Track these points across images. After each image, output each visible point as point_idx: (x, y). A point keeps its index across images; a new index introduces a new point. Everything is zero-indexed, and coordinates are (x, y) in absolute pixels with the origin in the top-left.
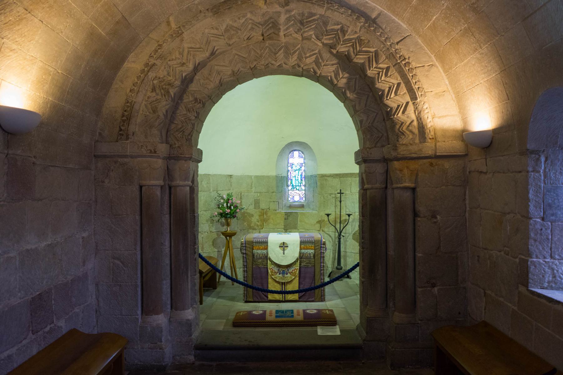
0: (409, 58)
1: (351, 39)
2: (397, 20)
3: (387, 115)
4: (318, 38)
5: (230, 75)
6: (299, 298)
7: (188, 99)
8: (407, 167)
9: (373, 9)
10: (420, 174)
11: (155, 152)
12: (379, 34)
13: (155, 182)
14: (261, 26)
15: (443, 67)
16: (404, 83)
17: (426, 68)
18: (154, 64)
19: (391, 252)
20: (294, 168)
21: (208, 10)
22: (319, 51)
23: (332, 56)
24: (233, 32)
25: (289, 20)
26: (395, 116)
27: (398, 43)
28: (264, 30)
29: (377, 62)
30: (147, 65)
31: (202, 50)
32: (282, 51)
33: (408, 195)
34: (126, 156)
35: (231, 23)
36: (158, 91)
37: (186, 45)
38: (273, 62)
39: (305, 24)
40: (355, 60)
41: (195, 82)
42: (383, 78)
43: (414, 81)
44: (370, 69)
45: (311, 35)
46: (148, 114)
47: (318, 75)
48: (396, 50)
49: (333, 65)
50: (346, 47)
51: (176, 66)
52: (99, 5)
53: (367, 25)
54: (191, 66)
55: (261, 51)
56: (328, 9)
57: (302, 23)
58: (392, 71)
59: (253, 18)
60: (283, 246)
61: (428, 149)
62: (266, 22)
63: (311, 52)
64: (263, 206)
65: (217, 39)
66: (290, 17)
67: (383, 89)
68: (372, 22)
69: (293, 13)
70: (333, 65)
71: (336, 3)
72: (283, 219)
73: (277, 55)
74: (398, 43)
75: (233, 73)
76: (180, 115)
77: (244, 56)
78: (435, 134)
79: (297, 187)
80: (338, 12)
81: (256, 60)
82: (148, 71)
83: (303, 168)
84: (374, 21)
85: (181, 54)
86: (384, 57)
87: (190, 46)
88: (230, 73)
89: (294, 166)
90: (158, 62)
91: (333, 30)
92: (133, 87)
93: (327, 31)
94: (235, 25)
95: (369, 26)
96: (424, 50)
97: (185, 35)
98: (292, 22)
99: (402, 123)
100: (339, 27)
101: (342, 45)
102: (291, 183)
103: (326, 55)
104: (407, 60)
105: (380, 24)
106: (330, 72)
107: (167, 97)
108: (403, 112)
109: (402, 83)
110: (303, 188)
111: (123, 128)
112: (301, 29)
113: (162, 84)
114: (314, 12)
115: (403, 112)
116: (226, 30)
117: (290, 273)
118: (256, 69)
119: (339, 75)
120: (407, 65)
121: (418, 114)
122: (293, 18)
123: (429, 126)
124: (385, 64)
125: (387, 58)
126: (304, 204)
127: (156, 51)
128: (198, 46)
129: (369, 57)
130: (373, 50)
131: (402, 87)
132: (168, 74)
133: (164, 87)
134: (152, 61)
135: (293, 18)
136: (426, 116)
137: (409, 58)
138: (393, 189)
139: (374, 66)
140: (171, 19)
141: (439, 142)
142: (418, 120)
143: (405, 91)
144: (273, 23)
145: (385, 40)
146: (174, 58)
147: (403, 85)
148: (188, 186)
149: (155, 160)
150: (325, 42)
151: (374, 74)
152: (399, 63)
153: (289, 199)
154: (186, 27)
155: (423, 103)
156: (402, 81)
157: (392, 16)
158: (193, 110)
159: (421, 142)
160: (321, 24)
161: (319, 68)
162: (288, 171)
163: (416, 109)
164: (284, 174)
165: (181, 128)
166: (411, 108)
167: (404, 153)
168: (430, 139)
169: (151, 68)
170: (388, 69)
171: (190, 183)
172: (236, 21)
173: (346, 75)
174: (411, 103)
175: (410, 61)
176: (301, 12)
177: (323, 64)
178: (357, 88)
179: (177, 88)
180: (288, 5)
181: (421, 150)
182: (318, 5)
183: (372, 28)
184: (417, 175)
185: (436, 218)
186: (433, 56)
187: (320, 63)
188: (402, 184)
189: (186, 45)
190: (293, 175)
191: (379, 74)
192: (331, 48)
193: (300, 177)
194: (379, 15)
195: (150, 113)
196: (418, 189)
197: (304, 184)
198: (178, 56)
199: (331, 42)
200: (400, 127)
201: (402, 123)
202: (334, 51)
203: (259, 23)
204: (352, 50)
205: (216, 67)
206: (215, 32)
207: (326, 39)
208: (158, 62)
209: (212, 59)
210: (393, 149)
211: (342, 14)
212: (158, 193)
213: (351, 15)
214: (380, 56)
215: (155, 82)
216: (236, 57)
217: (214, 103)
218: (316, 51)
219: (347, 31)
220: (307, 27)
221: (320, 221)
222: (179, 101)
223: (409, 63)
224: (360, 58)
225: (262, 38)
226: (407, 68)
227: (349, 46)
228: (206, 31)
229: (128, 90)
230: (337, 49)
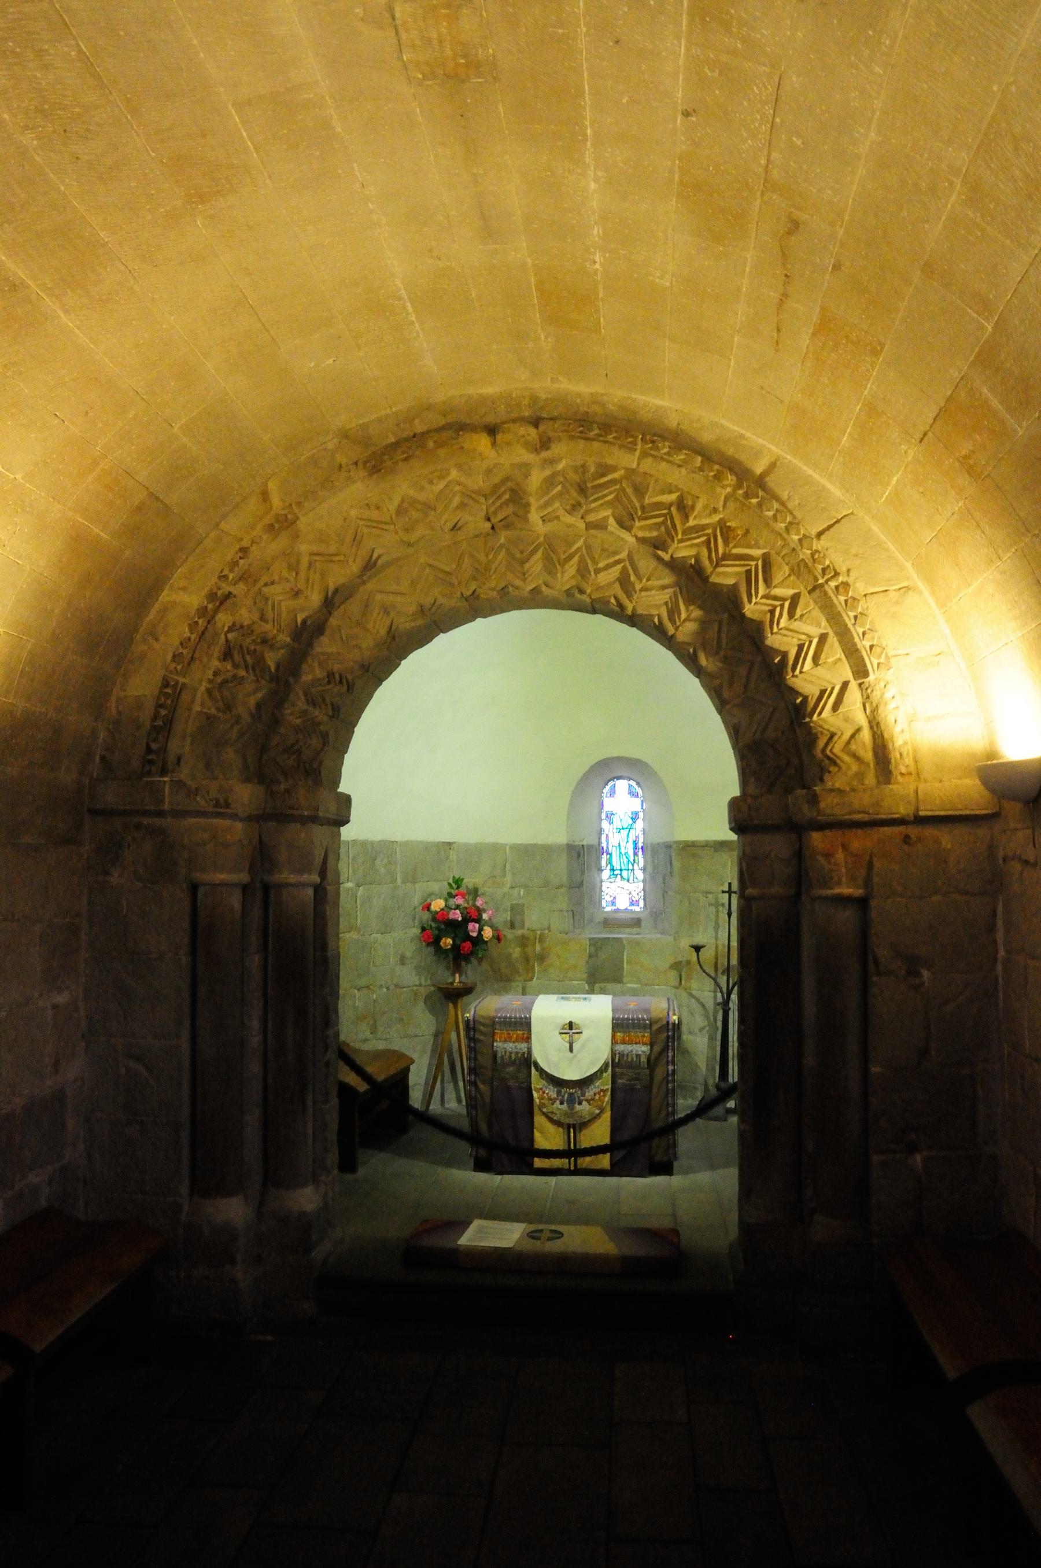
0: (848, 571)
1: (703, 527)
2: (816, 476)
3: (796, 713)
4: (621, 524)
5: (413, 614)
6: (612, 1164)
7: (312, 673)
8: (845, 847)
9: (758, 454)
10: (875, 863)
11: (227, 805)
12: (770, 514)
13: (227, 876)
14: (482, 500)
15: (933, 592)
16: (836, 634)
17: (893, 595)
18: (229, 595)
19: (809, 1061)
20: (617, 823)
21: (356, 463)
22: (630, 556)
23: (660, 567)
24: (414, 514)
25: (552, 484)
26: (815, 718)
27: (819, 535)
28: (492, 509)
29: (767, 581)
30: (212, 596)
31: (341, 558)
32: (539, 554)
33: (846, 916)
34: (160, 814)
35: (412, 493)
36: (237, 657)
37: (304, 548)
38: (518, 582)
39: (589, 493)
40: (714, 579)
41: (328, 631)
42: (782, 624)
43: (860, 630)
44: (750, 602)
45: (606, 518)
46: (213, 711)
47: (629, 613)
48: (813, 555)
49: (664, 587)
50: (692, 546)
51: (280, 598)
52: (90, 479)
53: (741, 492)
54: (315, 599)
55: (487, 555)
56: (644, 455)
57: (582, 490)
58: (807, 604)
59: (463, 479)
60: (570, 1030)
61: (899, 797)
62: (495, 488)
63: (608, 557)
65: (379, 532)
66: (554, 475)
67: (783, 649)
68: (753, 485)
69: (560, 467)
70: (664, 587)
71: (663, 438)
72: (586, 956)
73: (527, 566)
74: (819, 535)
75: (422, 610)
76: (292, 714)
77: (447, 569)
78: (916, 762)
79: (625, 874)
80: (669, 462)
81: (475, 579)
82: (216, 611)
83: (640, 824)
84: (761, 482)
85: (294, 568)
86: (786, 569)
87: (315, 549)
88: (413, 608)
89: (615, 818)
90: (239, 589)
91: (658, 505)
92: (181, 650)
93: (643, 508)
94: (422, 497)
95: (747, 495)
96: (887, 550)
97: (302, 523)
98: (559, 488)
99: (832, 735)
100: (673, 497)
101: (681, 541)
102: (609, 862)
103: (646, 564)
104: (841, 579)
105: (776, 489)
106: (657, 606)
107: (258, 672)
108: (836, 707)
109: (831, 634)
110: (640, 875)
111: (154, 746)
112: (580, 505)
113: (248, 640)
114: (611, 462)
115: (836, 707)
116: (400, 511)
117: (587, 1100)
118: (478, 598)
119: (679, 614)
120: (841, 590)
121: (873, 712)
122: (562, 479)
123: (899, 741)
124: (788, 587)
125: (792, 570)
126: (640, 916)
127: (234, 564)
128: (333, 549)
129: (748, 572)
130: (757, 552)
131: (832, 645)
132: (262, 618)
133: (252, 647)
134: (226, 588)
135: (562, 479)
136: (891, 719)
137: (848, 571)
138: (813, 899)
139: (761, 592)
140: (272, 486)
141: (926, 781)
142: (871, 727)
143: (839, 654)
144: (512, 490)
145: (787, 529)
146: (276, 577)
147: (833, 640)
148: (308, 885)
149: (228, 822)
150: (640, 534)
151: (761, 612)
152: (822, 585)
153: (604, 904)
154: (306, 504)
155: (882, 684)
156: (830, 631)
157: (805, 468)
158: (324, 700)
159: (879, 783)
160: (629, 491)
161: (629, 596)
162: (600, 831)
163: (867, 698)
164: (589, 840)
165: (293, 745)
166: (854, 695)
167: (837, 811)
168: (902, 774)
169: (221, 604)
170: (795, 600)
171: (315, 878)
172: (422, 488)
173: (697, 613)
174: (853, 685)
175: (851, 580)
176: (578, 463)
177: (638, 587)
178: (724, 642)
179: (282, 651)
180: (548, 449)
181: (877, 804)
182: (621, 447)
183: (754, 501)
184: (870, 865)
185: (918, 975)
186: (908, 565)
187: (633, 585)
188: (830, 888)
189: (304, 548)
190: (614, 841)
191: (772, 612)
192: (656, 547)
194: (773, 465)
195: (218, 709)
196: (873, 903)
197: (641, 864)
198: (285, 574)
199: (655, 534)
200: (827, 744)
201: (832, 735)
202: (666, 557)
203: (478, 492)
204: (705, 553)
205: (379, 597)
206: (375, 515)
207: (641, 528)
208: (239, 589)
209: (370, 578)
210: (808, 802)
211: (679, 466)
212: (235, 901)
213: (701, 469)
214: (774, 569)
215: (230, 636)
216: (428, 570)
217: (380, 681)
218: (624, 555)
219: (693, 507)
220: (595, 500)
221: (680, 962)
222: (291, 680)
223: (846, 585)
224: (724, 574)
225: (488, 525)
226: (842, 598)
227: (697, 545)
228: (353, 512)
229: (170, 656)
230: (670, 551)
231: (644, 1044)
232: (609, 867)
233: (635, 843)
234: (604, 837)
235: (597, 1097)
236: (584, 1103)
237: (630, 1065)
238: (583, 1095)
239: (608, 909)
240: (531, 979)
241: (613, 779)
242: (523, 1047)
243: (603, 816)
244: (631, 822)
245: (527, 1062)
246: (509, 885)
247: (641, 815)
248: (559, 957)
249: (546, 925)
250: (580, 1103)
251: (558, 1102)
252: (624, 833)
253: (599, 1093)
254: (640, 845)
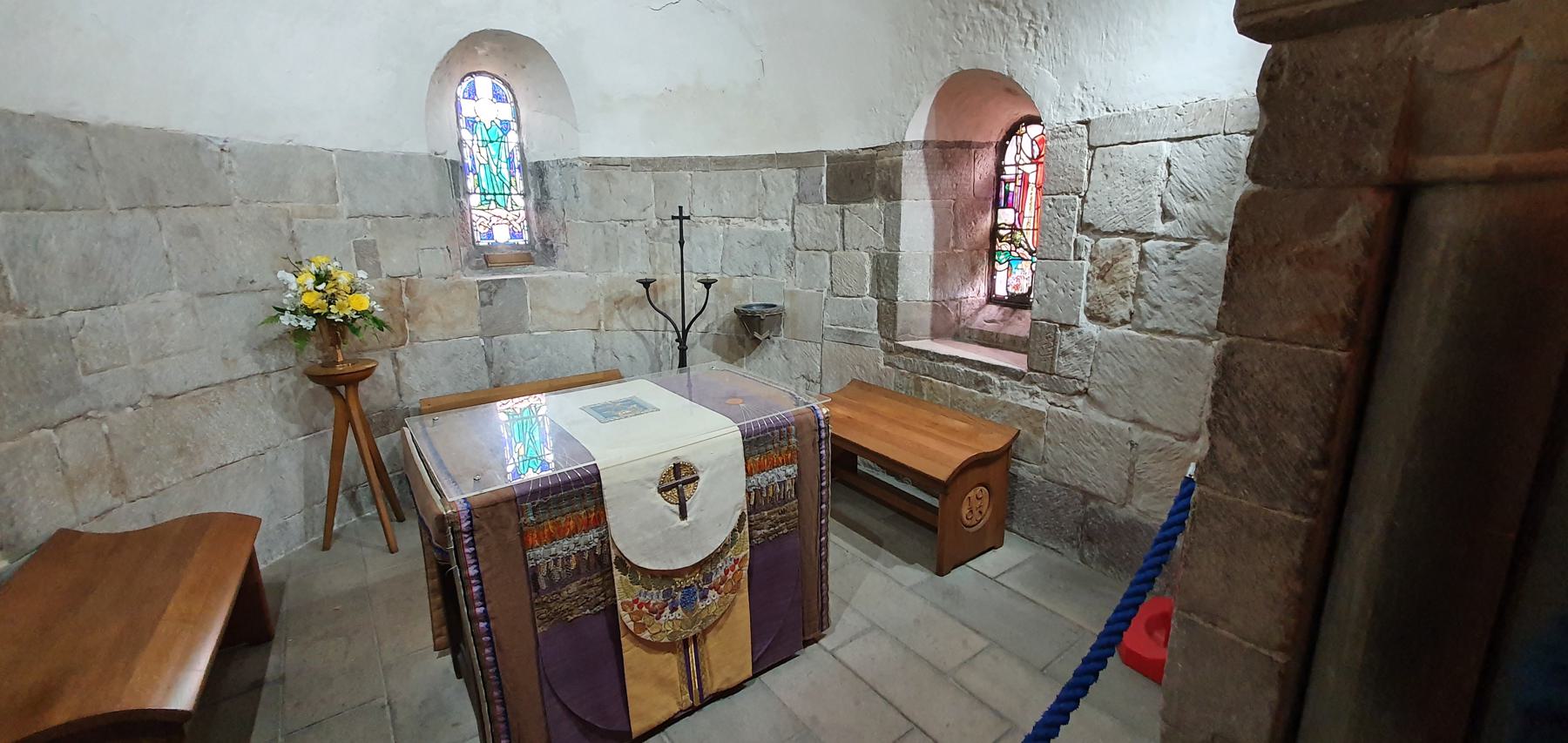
64: (395, 262)
79: (499, 198)
83: (512, 137)
110: (519, 201)
153: (477, 238)
162: (461, 142)
193: (504, 165)
197: (521, 188)
231: (788, 463)
233: (510, 160)
234: (466, 151)
235: (729, 576)
236: (712, 593)
237: (772, 503)
238: (707, 579)
240: (403, 343)
241: (470, 74)
242: (592, 536)
243: (462, 123)
245: (603, 562)
246: (346, 214)
247: (514, 126)
248: (438, 309)
249: (415, 269)
250: (704, 597)
251: (667, 610)
253: (733, 568)
254: (517, 163)
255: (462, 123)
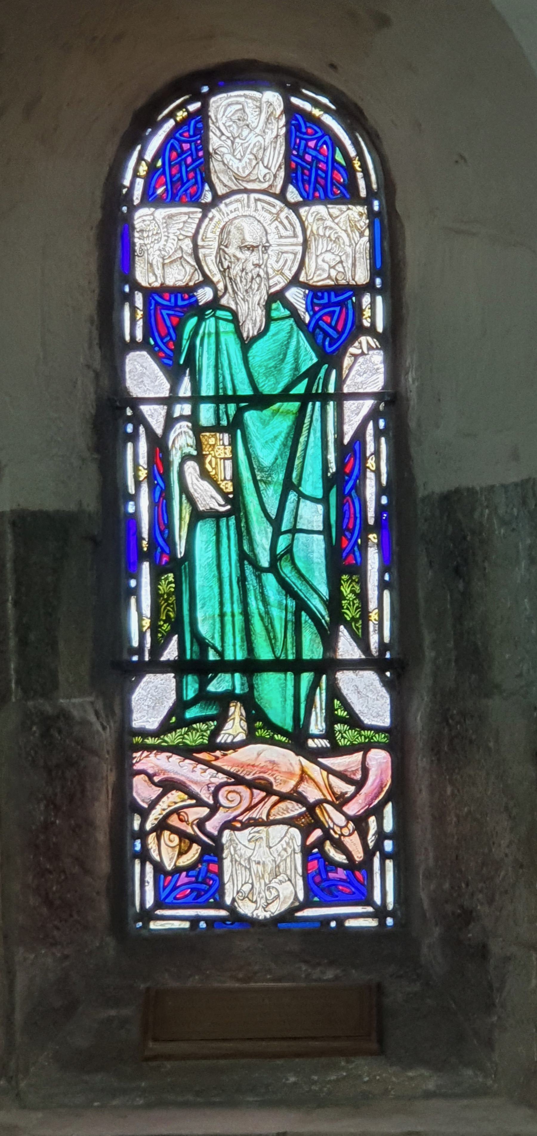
79: (275, 693)
83: (366, 369)
89: (212, 344)
110: (369, 697)
162: (113, 412)
193: (312, 515)
232: (171, 653)
234: (136, 456)
239: (172, 921)
243: (131, 323)
244: (309, 358)
247: (375, 311)
252: (267, 431)
255: (131, 323)
